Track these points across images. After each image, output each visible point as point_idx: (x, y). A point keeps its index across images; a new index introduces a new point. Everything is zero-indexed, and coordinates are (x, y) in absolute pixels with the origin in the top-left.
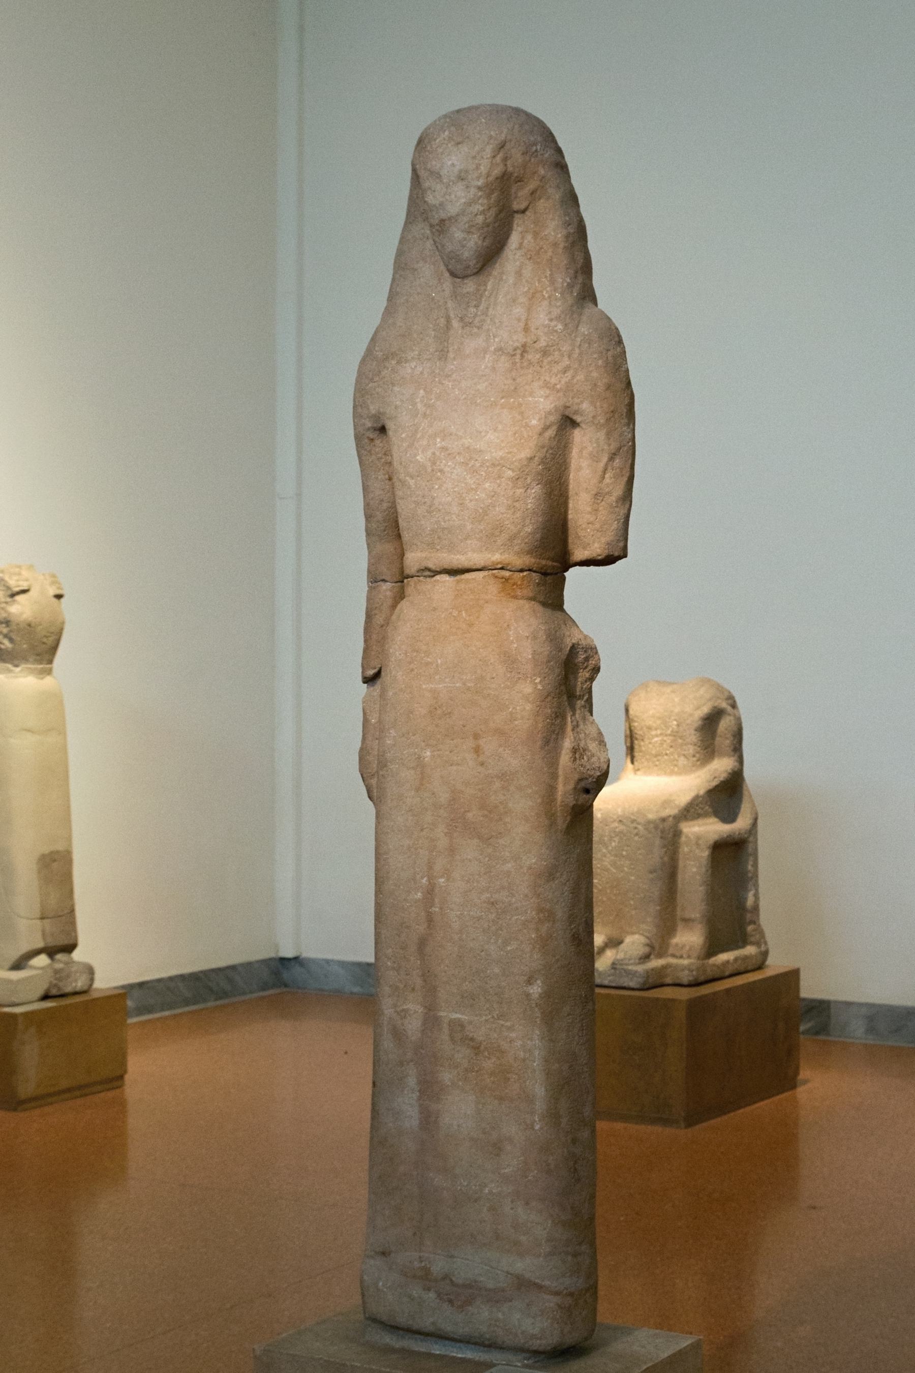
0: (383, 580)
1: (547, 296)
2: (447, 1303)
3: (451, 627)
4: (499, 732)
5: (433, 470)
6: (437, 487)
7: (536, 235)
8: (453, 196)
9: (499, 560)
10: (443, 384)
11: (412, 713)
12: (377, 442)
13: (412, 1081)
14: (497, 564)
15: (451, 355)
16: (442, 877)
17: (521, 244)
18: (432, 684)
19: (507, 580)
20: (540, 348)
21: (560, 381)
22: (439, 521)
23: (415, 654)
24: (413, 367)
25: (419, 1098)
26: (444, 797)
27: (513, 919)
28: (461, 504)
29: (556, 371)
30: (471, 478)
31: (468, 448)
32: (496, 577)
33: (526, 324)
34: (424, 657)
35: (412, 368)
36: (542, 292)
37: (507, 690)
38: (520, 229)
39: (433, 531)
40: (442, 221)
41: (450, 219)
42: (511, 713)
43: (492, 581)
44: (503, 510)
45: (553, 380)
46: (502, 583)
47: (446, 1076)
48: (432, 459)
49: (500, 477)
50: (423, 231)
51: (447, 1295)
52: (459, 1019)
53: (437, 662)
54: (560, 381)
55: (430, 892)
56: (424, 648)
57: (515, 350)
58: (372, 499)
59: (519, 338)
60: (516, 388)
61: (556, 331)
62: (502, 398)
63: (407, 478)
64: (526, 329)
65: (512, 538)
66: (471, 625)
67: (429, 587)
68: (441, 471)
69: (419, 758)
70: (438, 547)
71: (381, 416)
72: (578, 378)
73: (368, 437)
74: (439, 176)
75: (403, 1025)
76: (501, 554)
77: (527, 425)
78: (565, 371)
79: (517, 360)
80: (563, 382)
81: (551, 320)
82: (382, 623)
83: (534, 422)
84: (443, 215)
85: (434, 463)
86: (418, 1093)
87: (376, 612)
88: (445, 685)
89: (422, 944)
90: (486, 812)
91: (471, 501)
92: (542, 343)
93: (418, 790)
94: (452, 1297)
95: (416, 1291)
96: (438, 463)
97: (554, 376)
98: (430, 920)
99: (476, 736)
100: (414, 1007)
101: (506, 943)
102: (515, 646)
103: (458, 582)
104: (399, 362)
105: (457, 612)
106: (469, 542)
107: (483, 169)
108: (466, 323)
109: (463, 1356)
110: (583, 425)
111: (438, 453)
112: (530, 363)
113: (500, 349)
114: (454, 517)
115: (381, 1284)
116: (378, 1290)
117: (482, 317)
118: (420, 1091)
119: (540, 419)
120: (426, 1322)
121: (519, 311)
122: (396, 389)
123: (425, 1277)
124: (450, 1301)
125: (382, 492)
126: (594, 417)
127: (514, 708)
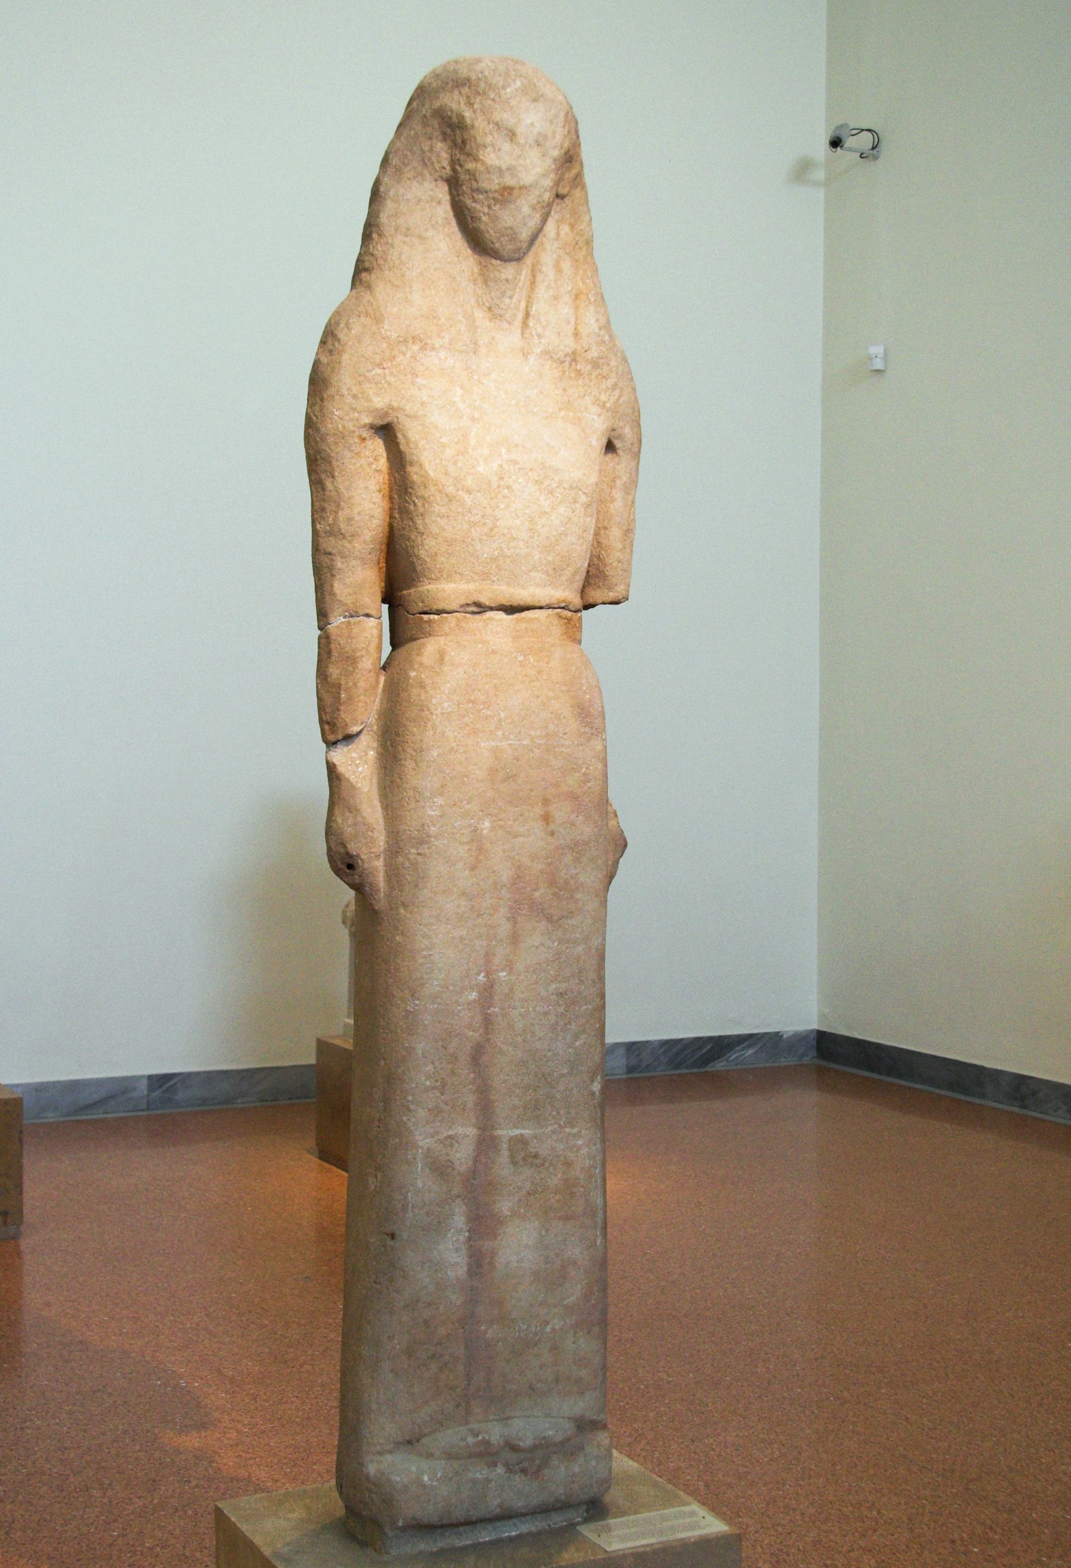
0: (368, 615)
1: (592, 300)
2: (519, 1474)
3: (516, 674)
4: (573, 797)
5: (499, 487)
6: (502, 506)
7: (572, 226)
8: (528, 162)
9: (563, 598)
10: (483, 384)
11: (467, 776)
12: (369, 443)
13: (459, 1220)
14: (563, 601)
15: (483, 350)
16: (503, 970)
17: (558, 234)
18: (493, 741)
19: (569, 620)
20: (592, 358)
21: (609, 400)
22: (501, 548)
23: (470, 705)
24: (443, 358)
25: (469, 1239)
26: (506, 874)
27: (582, 1009)
28: (531, 530)
29: (604, 387)
30: (545, 500)
31: (542, 464)
32: (560, 617)
33: (576, 329)
34: (483, 709)
35: (440, 359)
36: (587, 295)
37: (581, 748)
38: (556, 217)
39: (494, 559)
40: (509, 189)
41: (521, 188)
42: (584, 774)
43: (556, 621)
44: (574, 540)
45: (603, 398)
46: (565, 624)
47: (504, 1206)
48: (499, 473)
49: (575, 502)
50: (432, 193)
51: (518, 1464)
52: (521, 1134)
53: (500, 715)
54: (609, 400)
55: (488, 991)
56: (482, 698)
57: (565, 356)
58: (359, 513)
59: (569, 344)
60: (569, 401)
61: (604, 342)
62: (560, 410)
63: (460, 493)
64: (576, 334)
65: (575, 573)
66: (540, 672)
67: (481, 625)
68: (508, 487)
69: (476, 830)
70: (495, 579)
71: (390, 412)
72: (623, 398)
73: (360, 436)
74: (512, 135)
75: (447, 1154)
76: (563, 590)
77: (591, 446)
78: (615, 386)
79: (566, 369)
80: (611, 401)
81: (600, 329)
82: (370, 667)
83: (594, 442)
84: (509, 181)
85: (502, 478)
86: (467, 1234)
87: (364, 652)
88: (510, 742)
89: (478, 1052)
90: (556, 890)
91: (543, 526)
92: (594, 353)
93: (473, 868)
94: (526, 1464)
95: (479, 1472)
96: (506, 478)
97: (603, 393)
98: (488, 1022)
99: (546, 802)
100: (467, 1131)
101: (576, 1037)
102: (588, 697)
103: (517, 620)
104: (423, 348)
105: (523, 657)
106: (533, 574)
107: (559, 138)
108: (493, 312)
109: (518, 1533)
110: (620, 452)
111: (506, 467)
112: (579, 373)
113: (547, 354)
114: (521, 543)
115: (426, 1478)
116: (424, 1486)
117: (514, 311)
118: (469, 1231)
119: (598, 439)
120: (493, 1504)
121: (566, 310)
122: (419, 380)
123: (486, 1453)
124: (524, 1471)
125: (372, 506)
126: (632, 444)
127: (587, 768)
